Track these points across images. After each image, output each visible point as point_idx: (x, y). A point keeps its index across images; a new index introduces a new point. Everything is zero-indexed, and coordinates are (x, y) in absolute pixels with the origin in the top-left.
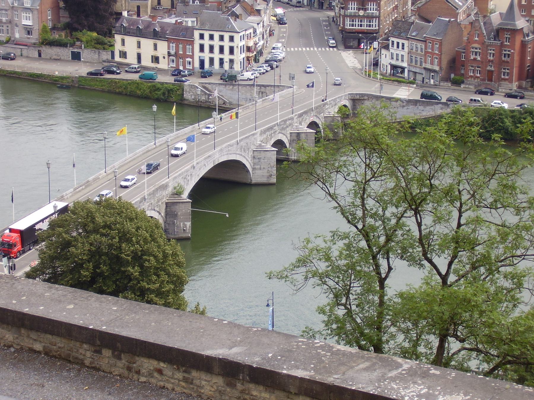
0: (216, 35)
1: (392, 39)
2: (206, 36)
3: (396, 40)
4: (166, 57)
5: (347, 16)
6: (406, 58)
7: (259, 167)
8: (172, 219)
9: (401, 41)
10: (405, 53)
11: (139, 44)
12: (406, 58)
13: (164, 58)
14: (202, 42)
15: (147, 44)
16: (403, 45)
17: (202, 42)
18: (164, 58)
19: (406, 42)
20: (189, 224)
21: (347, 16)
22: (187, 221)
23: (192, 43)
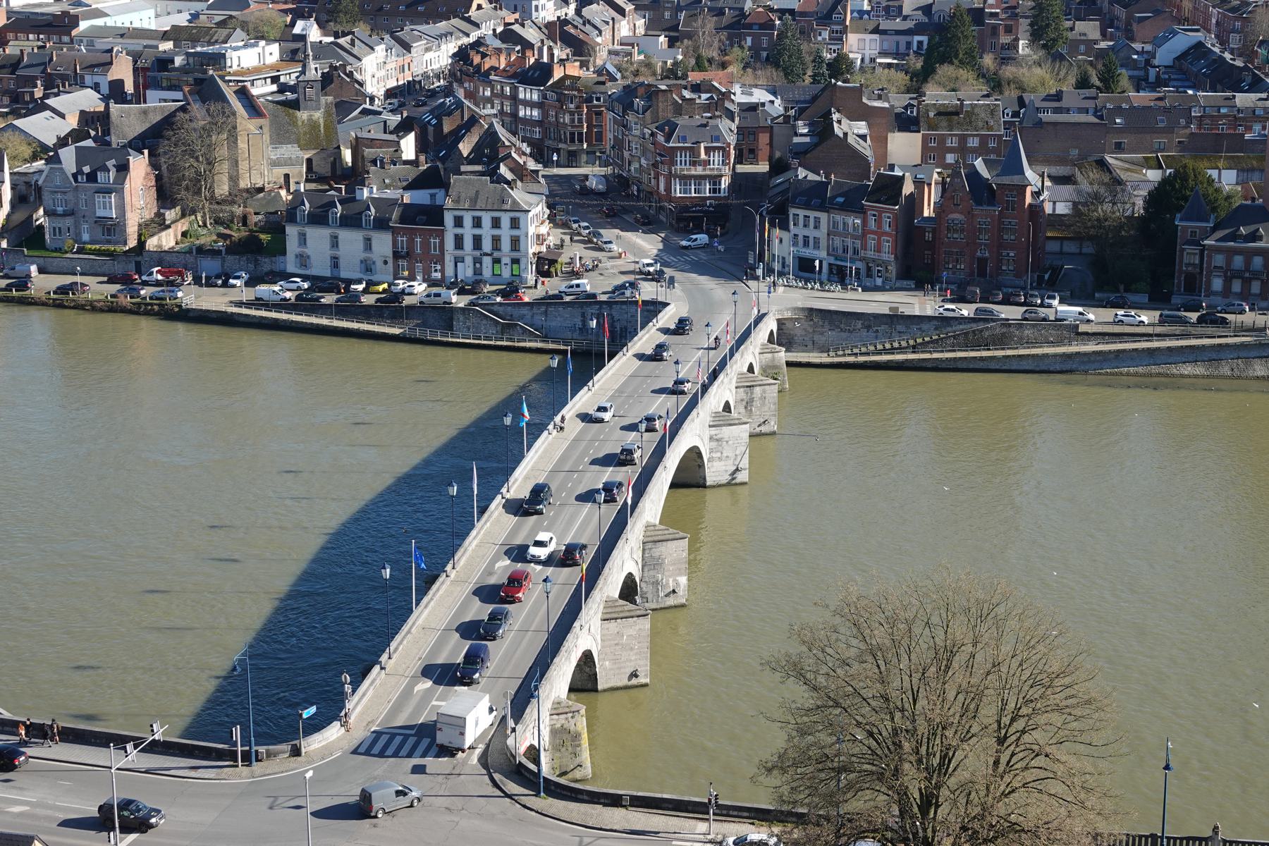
0: (486, 219)
1: (792, 211)
2: (468, 221)
3: (802, 213)
4: (390, 261)
5: (676, 176)
6: (823, 243)
7: (719, 455)
8: (652, 573)
9: (812, 214)
10: (822, 233)
11: (368, 241)
12: (823, 243)
13: (386, 262)
14: (459, 231)
15: (351, 240)
16: (817, 220)
17: (459, 231)
18: (386, 262)
19: (823, 217)
20: (683, 580)
21: (676, 176)
22: (680, 575)
23: (441, 234)
